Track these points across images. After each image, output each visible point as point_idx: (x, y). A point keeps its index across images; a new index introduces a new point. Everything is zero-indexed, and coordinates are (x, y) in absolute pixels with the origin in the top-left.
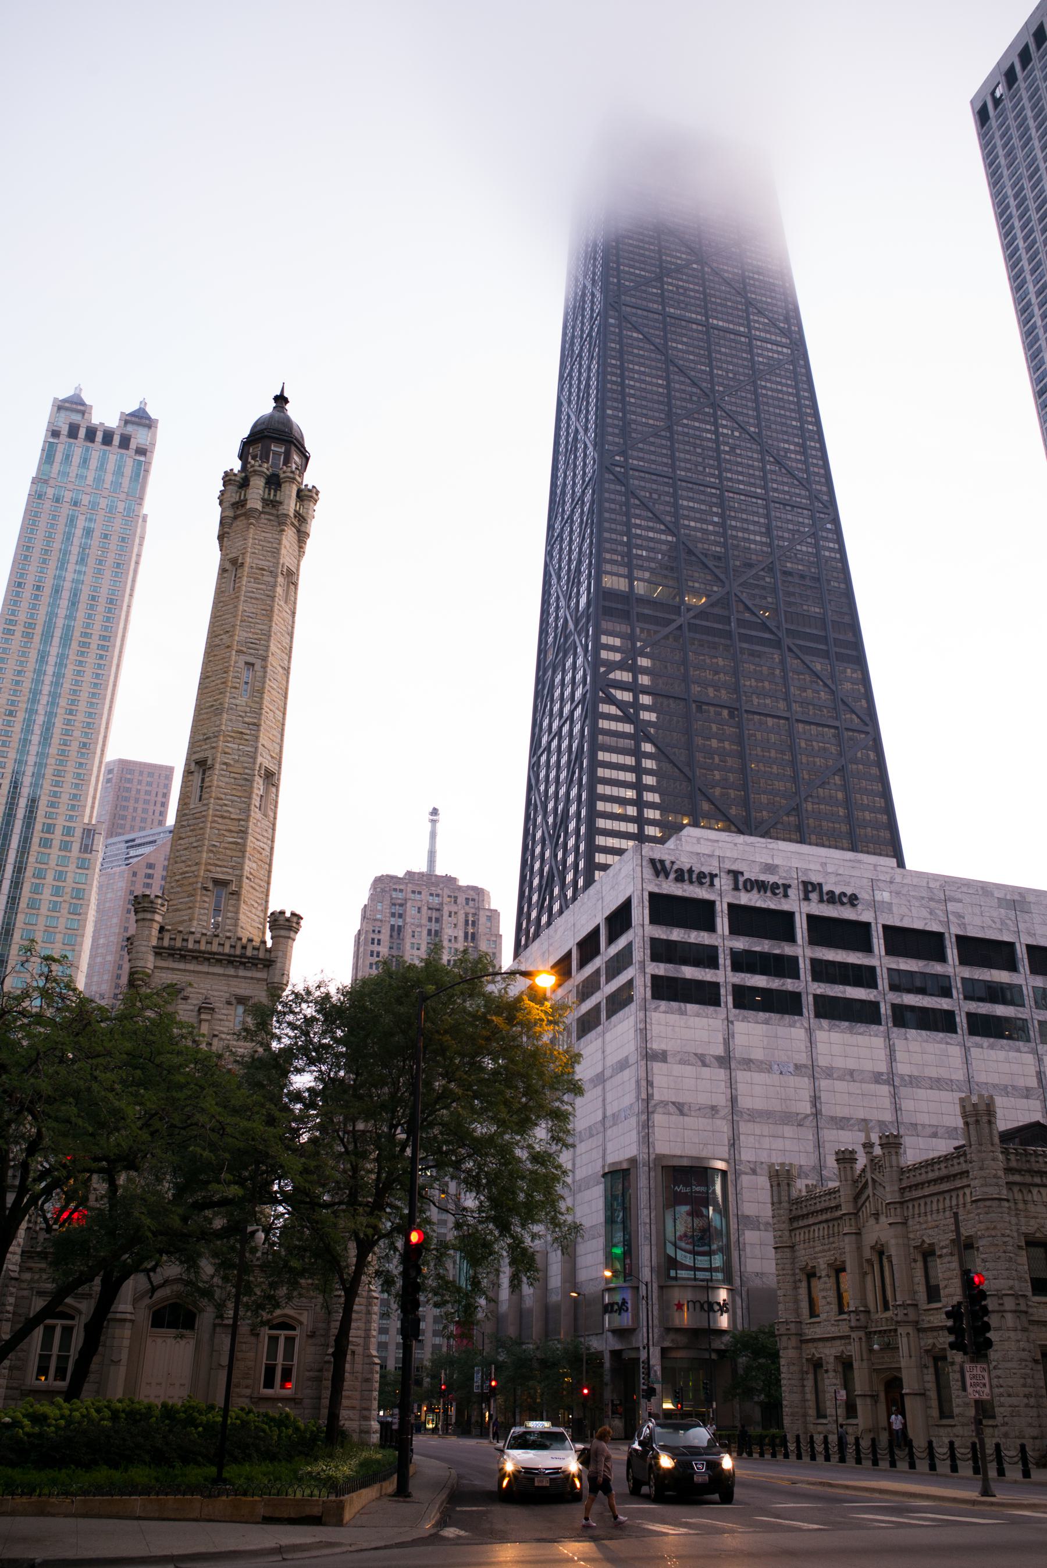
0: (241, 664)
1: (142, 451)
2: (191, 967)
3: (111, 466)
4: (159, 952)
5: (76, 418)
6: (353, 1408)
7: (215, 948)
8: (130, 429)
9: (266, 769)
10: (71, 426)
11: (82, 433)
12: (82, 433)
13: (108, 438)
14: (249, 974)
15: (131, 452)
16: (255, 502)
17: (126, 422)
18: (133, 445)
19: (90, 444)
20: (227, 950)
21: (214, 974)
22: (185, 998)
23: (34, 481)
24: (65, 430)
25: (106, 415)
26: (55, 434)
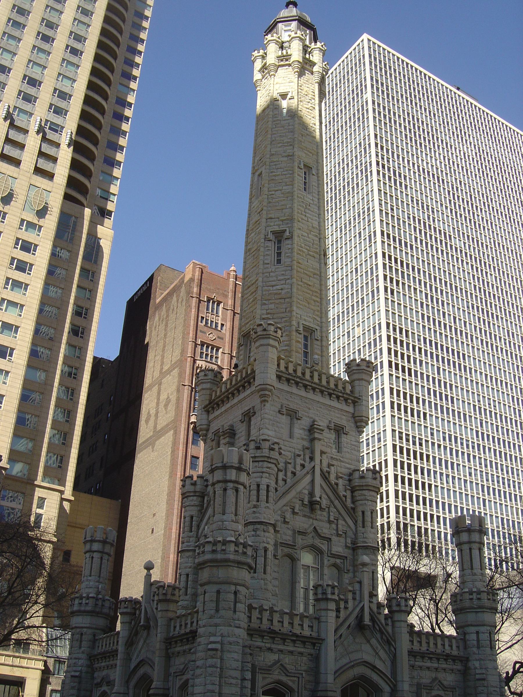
2: (223, 409)
9: (274, 233)
21: (234, 405)
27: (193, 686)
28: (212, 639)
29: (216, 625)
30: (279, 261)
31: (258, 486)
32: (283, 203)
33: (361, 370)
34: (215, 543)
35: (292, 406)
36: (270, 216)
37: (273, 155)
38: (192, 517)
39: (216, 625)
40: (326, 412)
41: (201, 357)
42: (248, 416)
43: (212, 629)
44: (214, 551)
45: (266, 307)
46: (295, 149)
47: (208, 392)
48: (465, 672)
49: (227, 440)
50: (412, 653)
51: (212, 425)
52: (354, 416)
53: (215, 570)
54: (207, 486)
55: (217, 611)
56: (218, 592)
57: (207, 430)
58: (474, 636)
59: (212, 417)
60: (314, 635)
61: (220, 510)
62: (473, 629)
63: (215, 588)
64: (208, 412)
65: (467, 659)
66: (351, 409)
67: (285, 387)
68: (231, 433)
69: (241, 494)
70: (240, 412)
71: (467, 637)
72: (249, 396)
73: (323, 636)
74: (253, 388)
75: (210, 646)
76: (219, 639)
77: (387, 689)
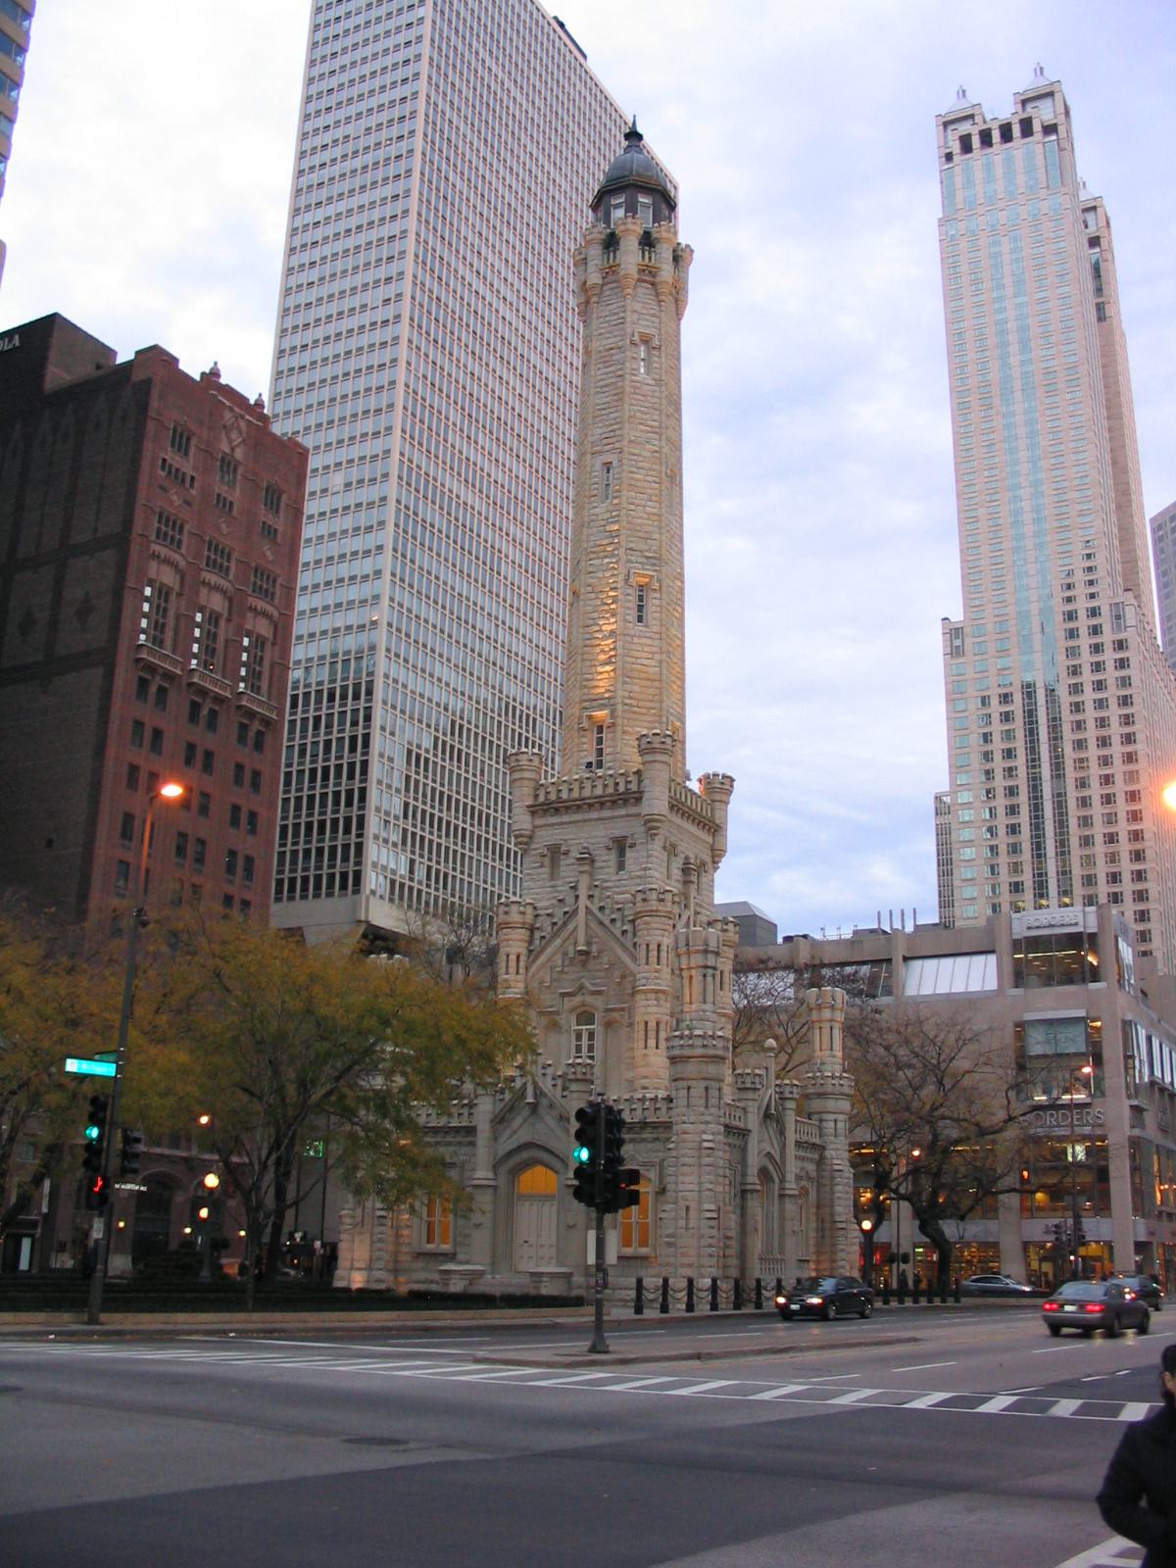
0: (598, 466)
1: (1050, 129)
2: (566, 818)
3: (1019, 165)
4: (534, 810)
5: (965, 128)
6: (690, 1266)
7: (587, 793)
8: (1030, 110)
10: (969, 137)
11: (976, 142)
12: (976, 142)
13: (1006, 133)
14: (623, 812)
15: (1038, 136)
16: (594, 278)
17: (1024, 102)
18: (1037, 127)
19: (989, 150)
20: (599, 791)
21: (591, 820)
22: (567, 853)
23: (942, 223)
24: (956, 147)
25: (1001, 108)
26: (949, 157)
27: (676, 1183)
28: (705, 1137)
29: (707, 1123)
30: (640, 619)
31: (659, 946)
32: (647, 529)
33: (719, 787)
34: (703, 1037)
35: (673, 839)
36: (631, 545)
37: (631, 441)
38: (518, 957)
39: (707, 1123)
40: (692, 844)
41: (158, 537)
42: (621, 846)
43: (702, 1127)
44: (704, 1046)
45: (628, 687)
46: (663, 443)
47: (532, 784)
48: (820, 1162)
49: (586, 868)
50: (798, 1144)
51: (540, 833)
52: (713, 850)
53: (703, 1066)
54: (537, 916)
55: (707, 1107)
56: (707, 1088)
57: (531, 837)
58: (832, 1124)
59: (539, 822)
60: (742, 1125)
61: (701, 998)
62: (832, 1117)
63: (703, 1084)
64: (533, 813)
65: (824, 1148)
66: (710, 839)
67: (677, 819)
68: (588, 859)
69: (709, 979)
70: (603, 833)
71: (824, 1124)
72: (622, 817)
73: (750, 1127)
74: (633, 810)
75: (706, 1144)
76: (710, 1137)
77: (777, 1180)
